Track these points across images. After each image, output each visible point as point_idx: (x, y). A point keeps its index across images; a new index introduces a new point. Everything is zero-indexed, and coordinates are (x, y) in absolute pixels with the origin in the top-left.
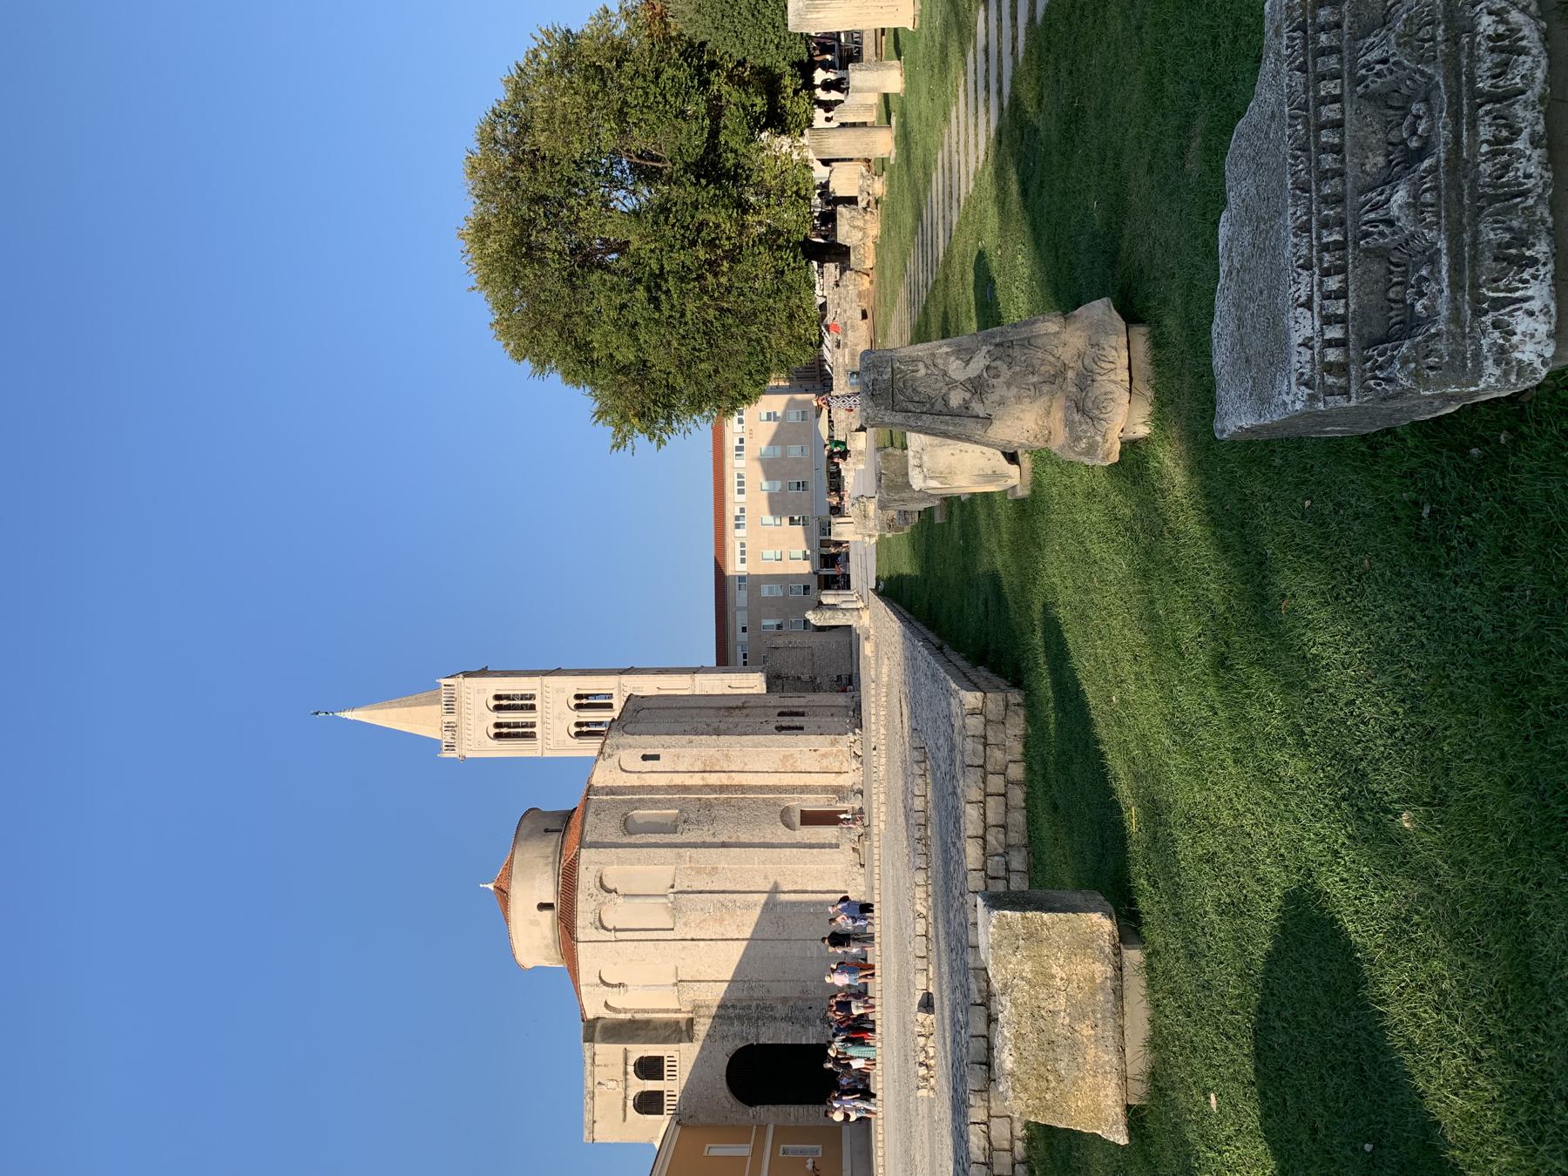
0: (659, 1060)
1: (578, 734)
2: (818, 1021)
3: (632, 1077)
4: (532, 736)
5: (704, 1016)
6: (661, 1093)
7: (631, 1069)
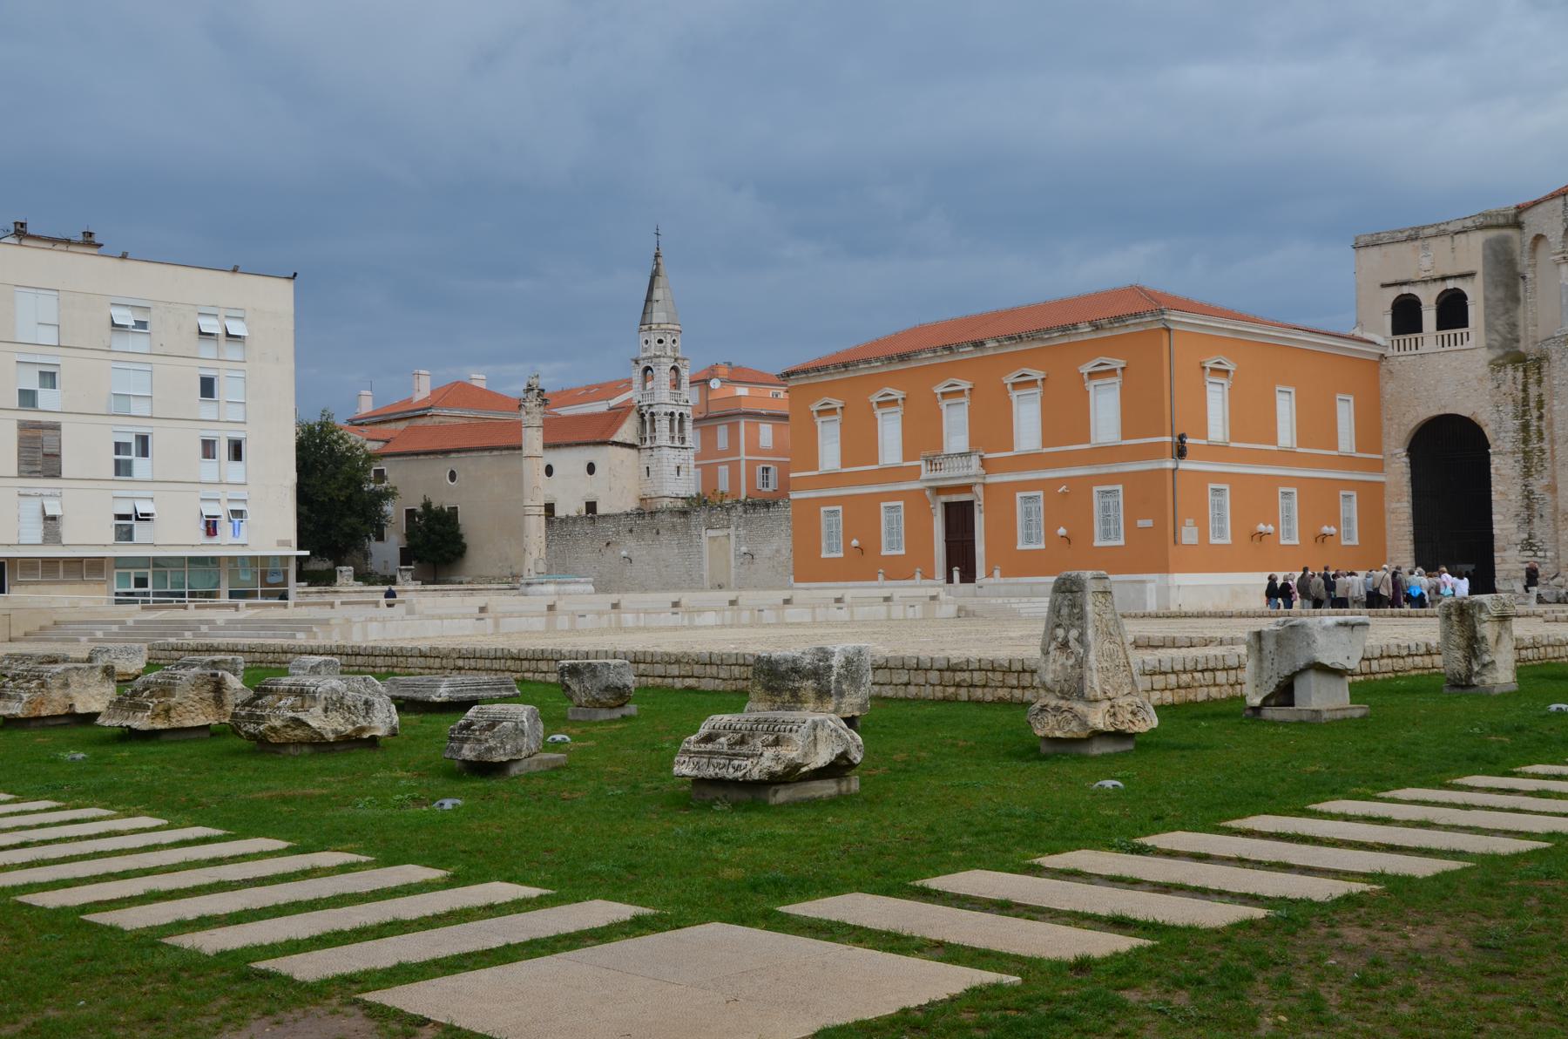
0: (1463, 323)
3: (1438, 289)
5: (1525, 376)
6: (1420, 330)
7: (1450, 284)
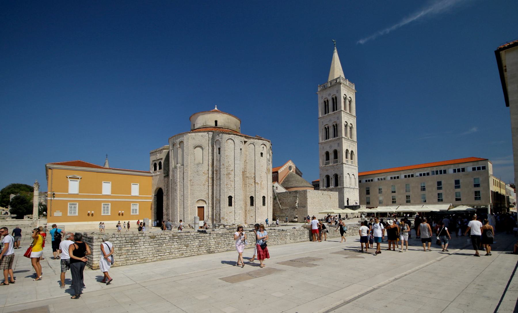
1: (325, 128)
2: (167, 213)
4: (326, 113)
